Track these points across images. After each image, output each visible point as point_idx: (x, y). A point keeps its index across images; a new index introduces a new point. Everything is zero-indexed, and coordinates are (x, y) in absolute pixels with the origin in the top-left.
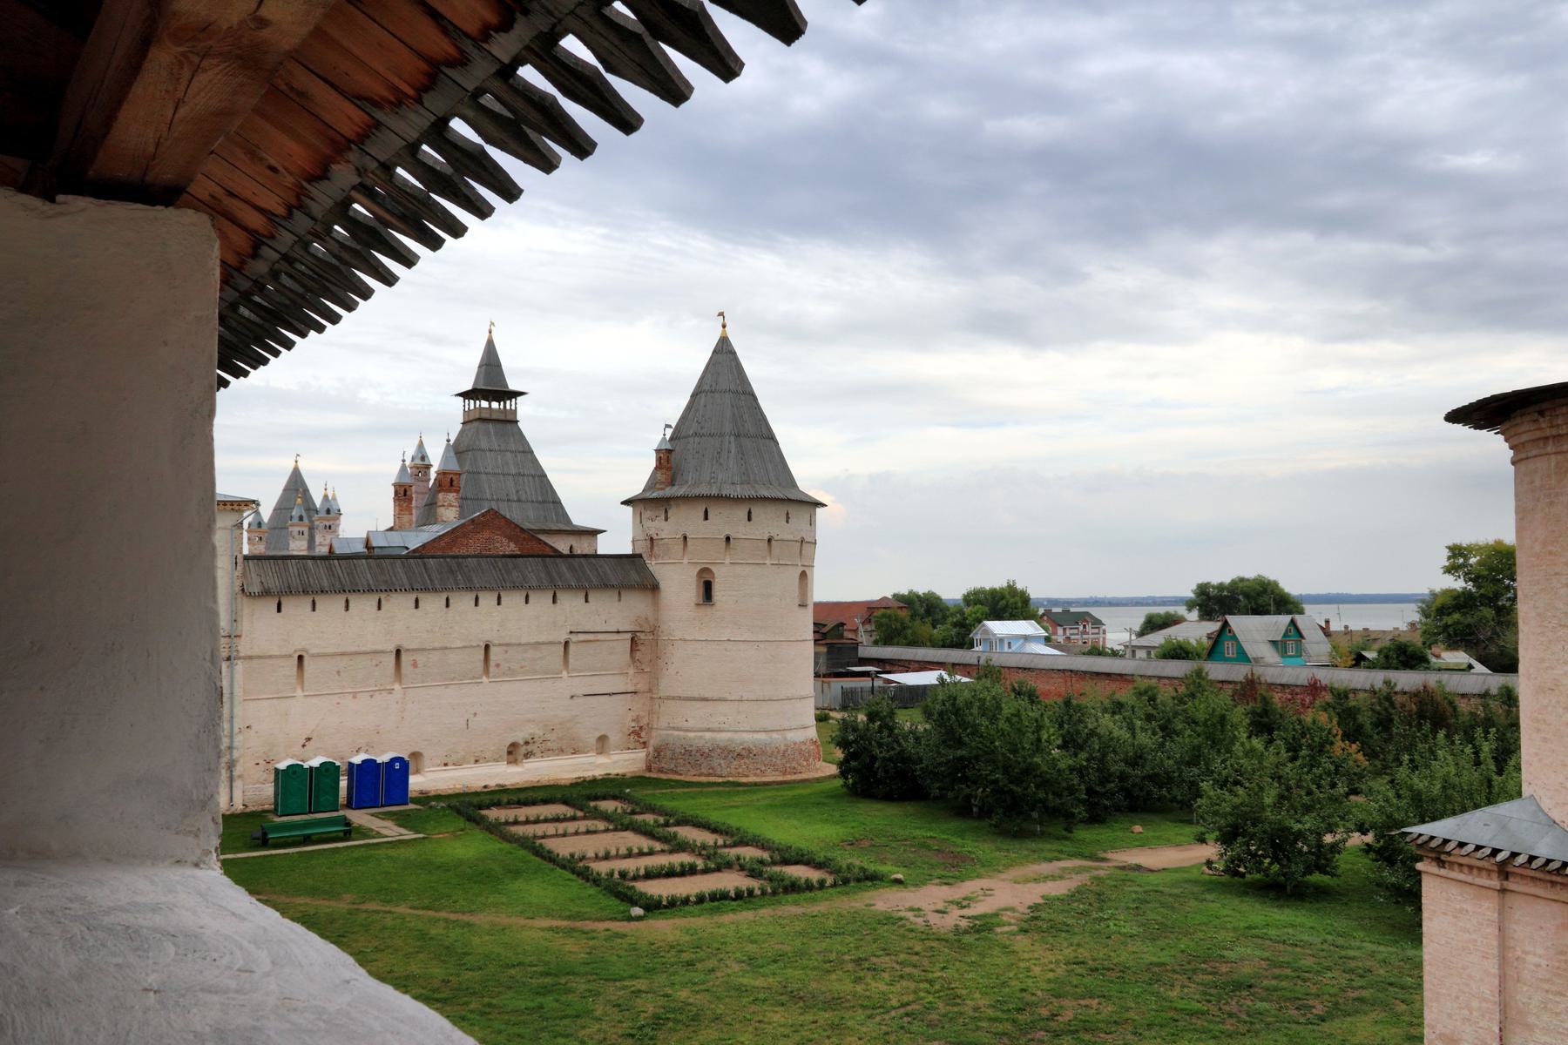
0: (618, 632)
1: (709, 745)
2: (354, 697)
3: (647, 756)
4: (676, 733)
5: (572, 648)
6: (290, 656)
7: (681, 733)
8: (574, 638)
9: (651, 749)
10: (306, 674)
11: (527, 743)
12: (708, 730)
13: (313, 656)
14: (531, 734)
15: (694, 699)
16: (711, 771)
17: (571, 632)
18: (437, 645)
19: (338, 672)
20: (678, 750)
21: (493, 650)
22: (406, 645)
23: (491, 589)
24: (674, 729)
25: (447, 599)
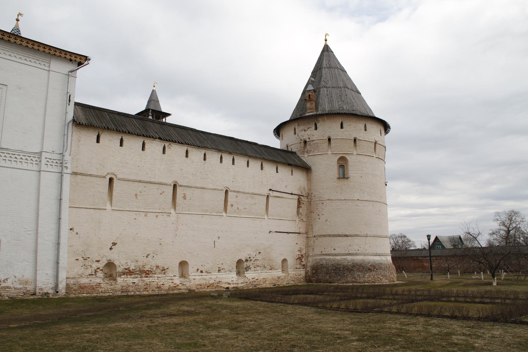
0: (292, 194)
1: (350, 263)
2: (146, 216)
3: (306, 273)
4: (327, 257)
5: (270, 199)
6: (104, 177)
7: (331, 257)
8: (271, 192)
9: (309, 269)
10: (114, 193)
11: (247, 260)
12: (349, 254)
13: (120, 179)
14: (249, 255)
15: (339, 236)
16: (354, 279)
17: (270, 190)
18: (198, 185)
19: (136, 195)
20: (330, 268)
21: (230, 193)
22: (180, 182)
23: (230, 153)
24: (326, 255)
25: (205, 155)
